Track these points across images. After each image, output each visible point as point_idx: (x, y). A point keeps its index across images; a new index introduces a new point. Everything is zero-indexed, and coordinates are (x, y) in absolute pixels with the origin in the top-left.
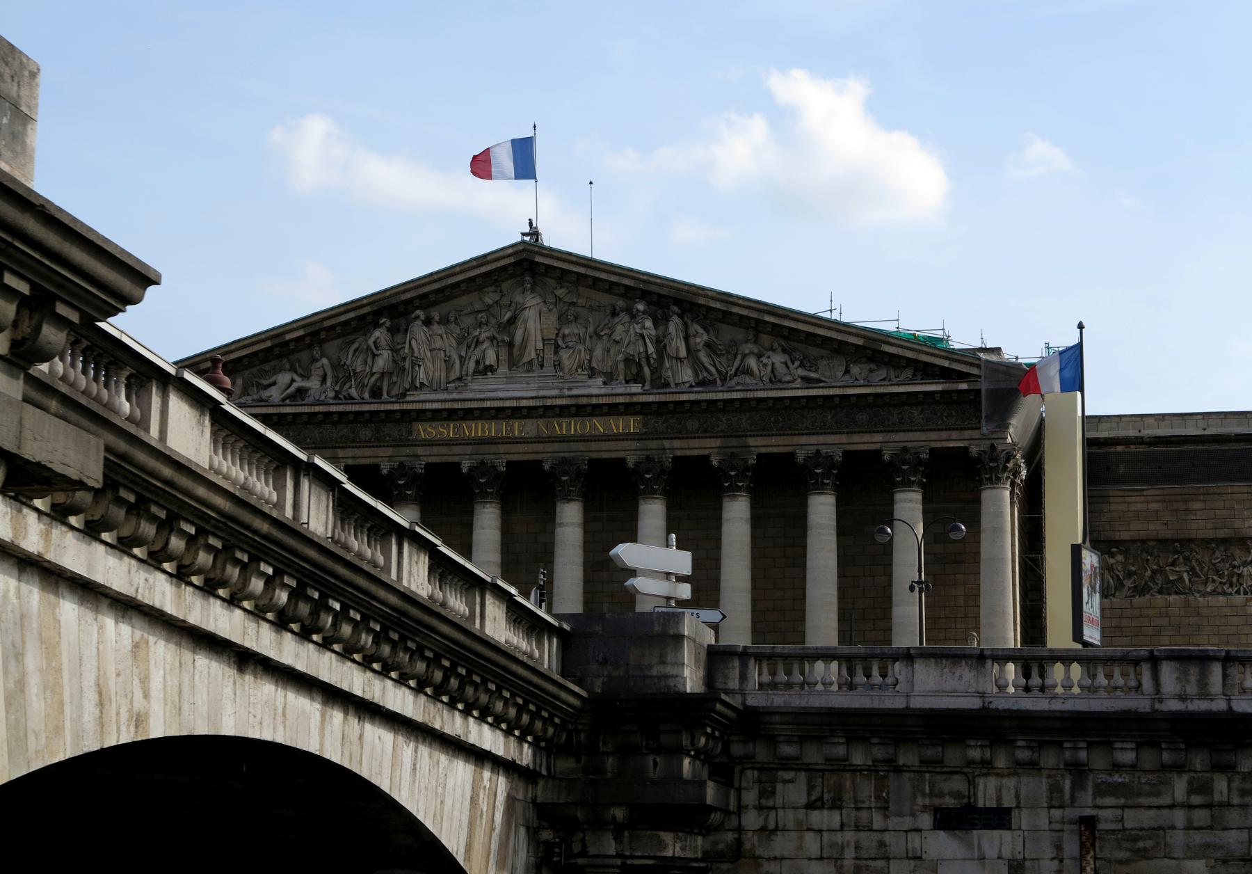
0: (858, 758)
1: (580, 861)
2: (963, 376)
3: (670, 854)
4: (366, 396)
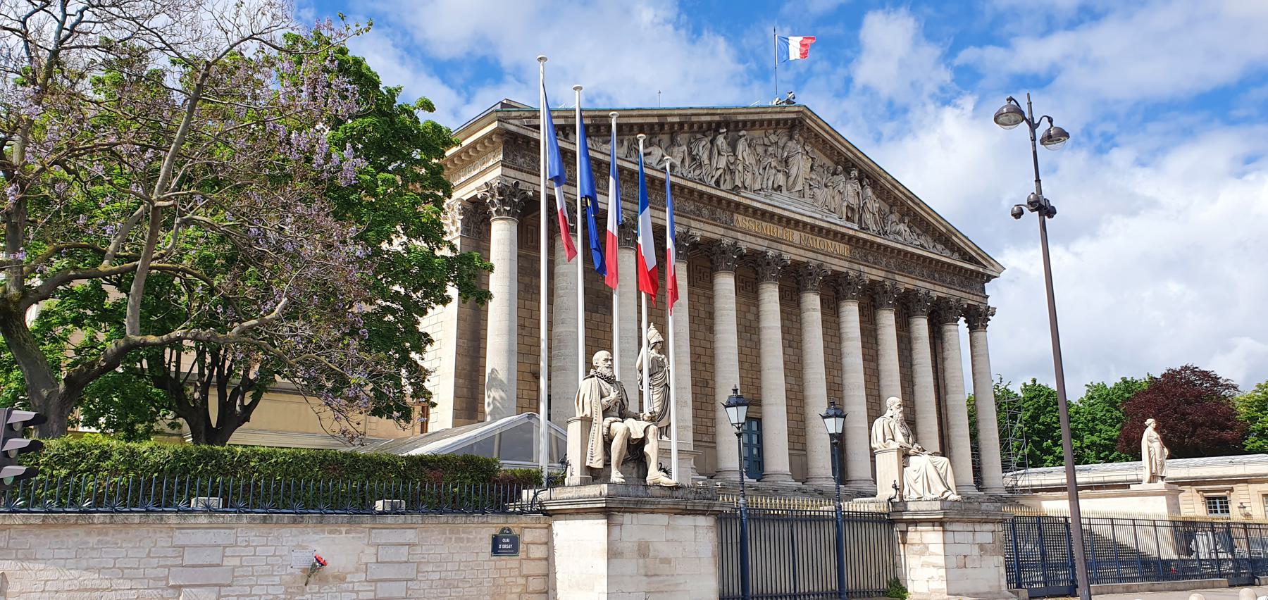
2: (977, 263)
4: (713, 183)
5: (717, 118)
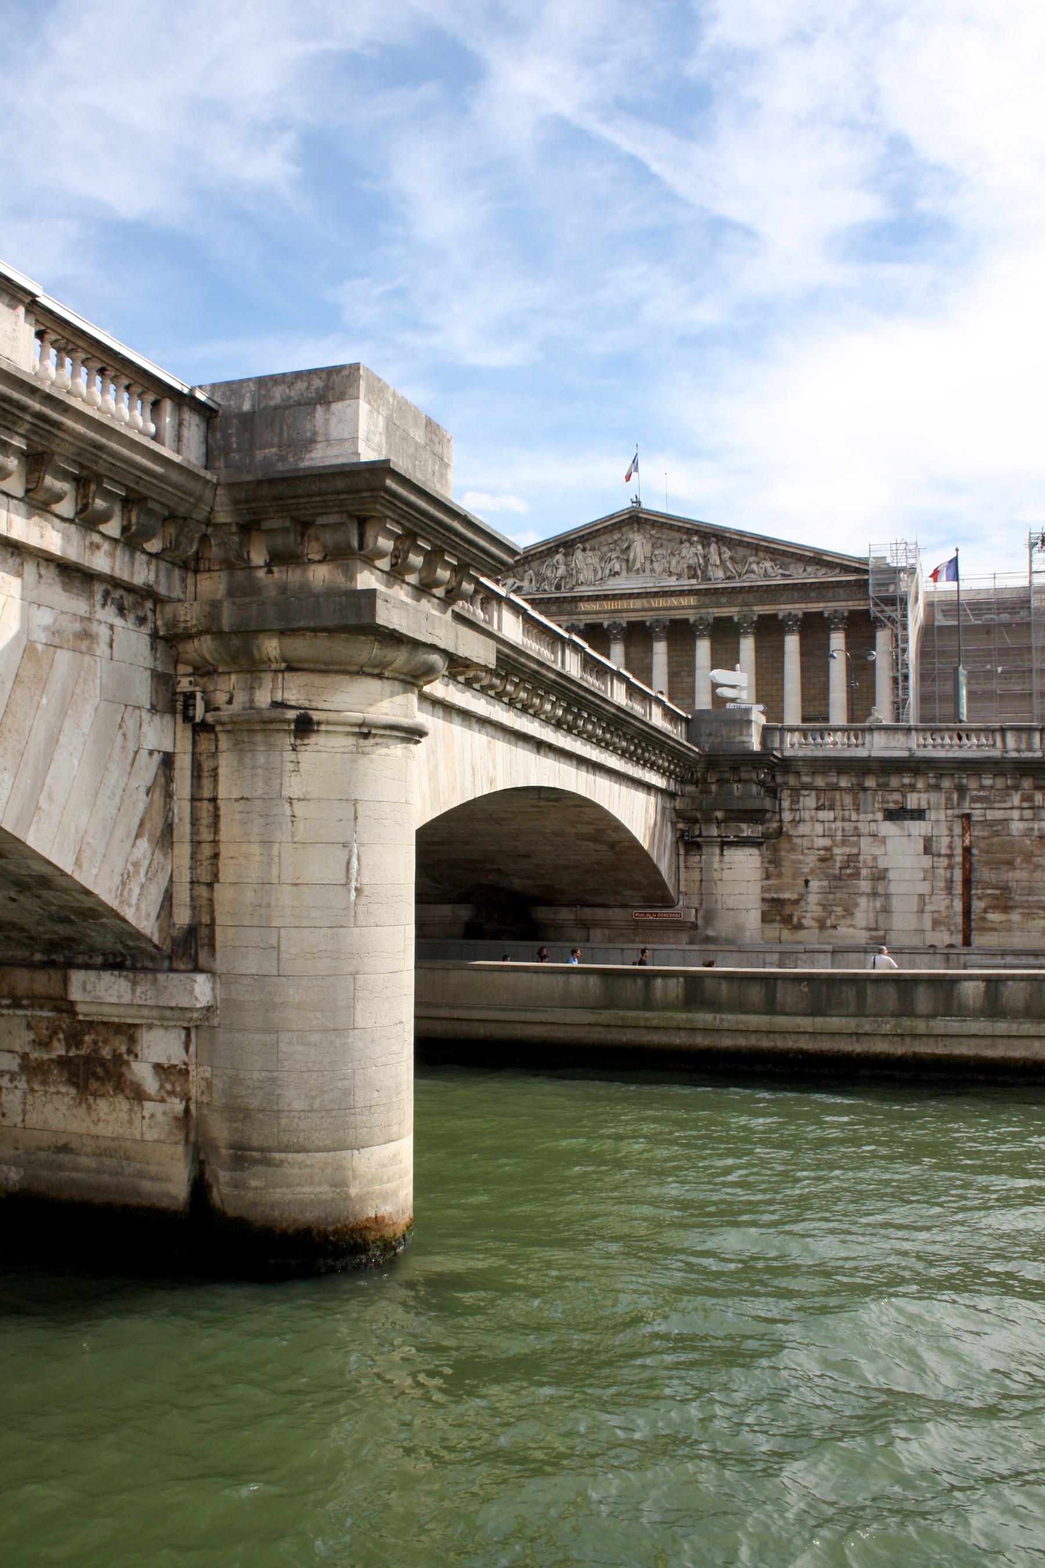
0: (844, 783)
1: (699, 839)
3: (745, 835)
4: (553, 589)
5: (552, 544)
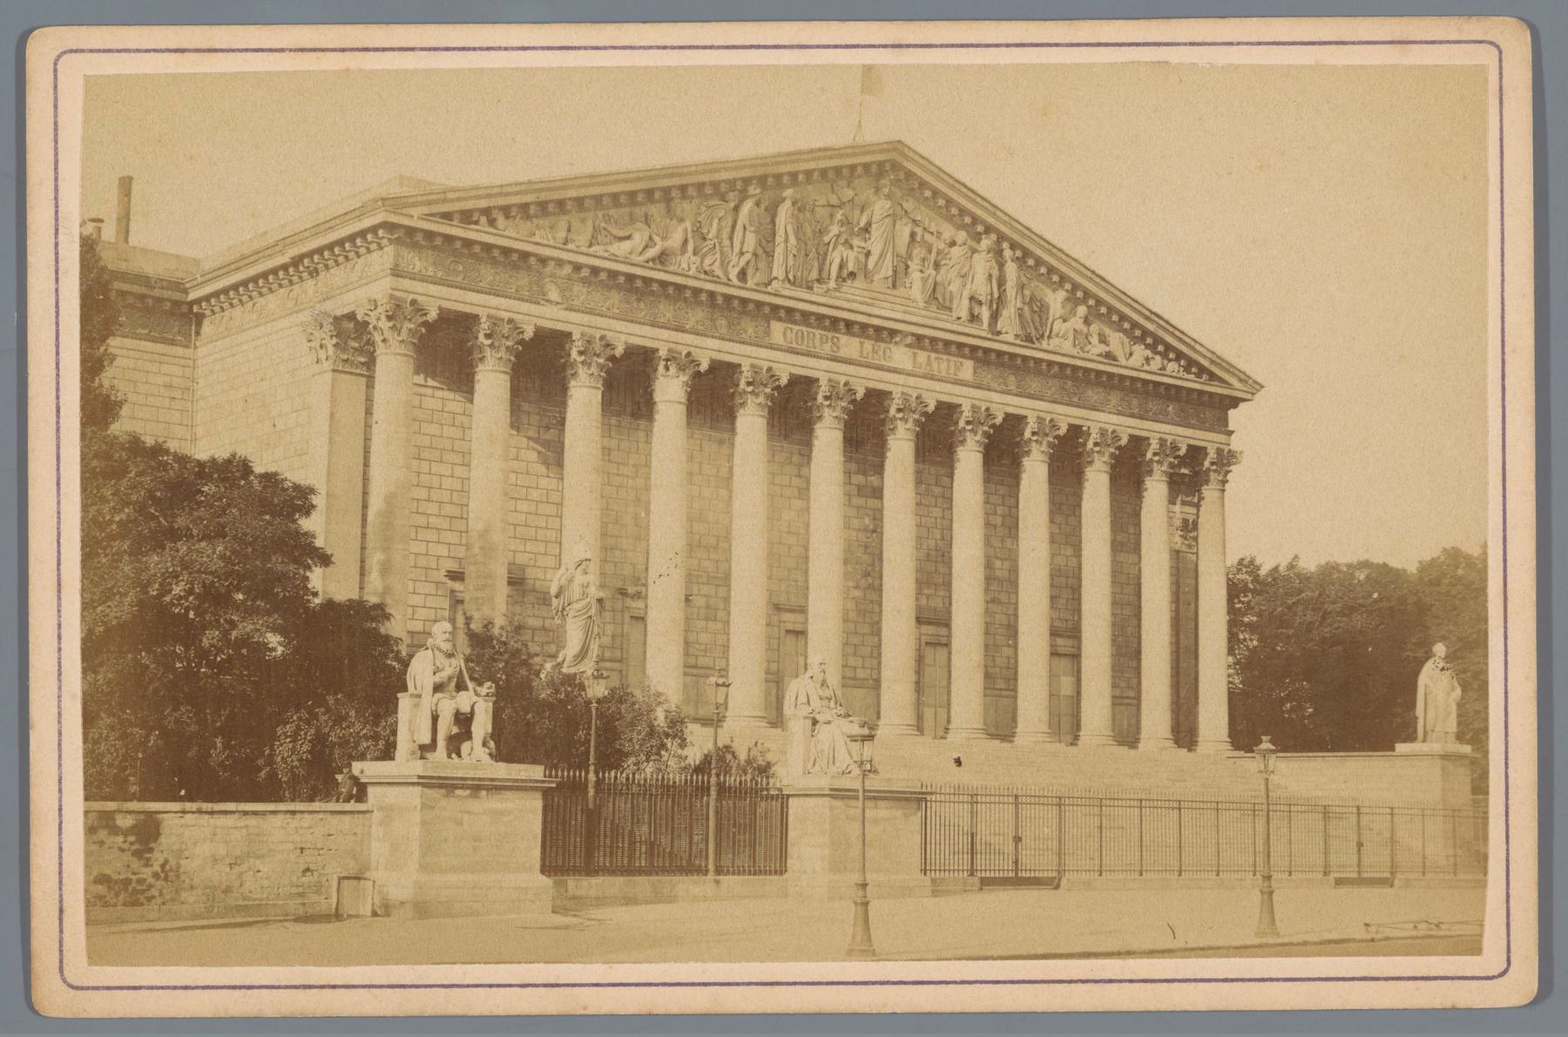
4: (733, 274)
